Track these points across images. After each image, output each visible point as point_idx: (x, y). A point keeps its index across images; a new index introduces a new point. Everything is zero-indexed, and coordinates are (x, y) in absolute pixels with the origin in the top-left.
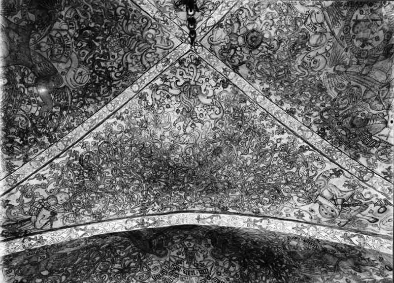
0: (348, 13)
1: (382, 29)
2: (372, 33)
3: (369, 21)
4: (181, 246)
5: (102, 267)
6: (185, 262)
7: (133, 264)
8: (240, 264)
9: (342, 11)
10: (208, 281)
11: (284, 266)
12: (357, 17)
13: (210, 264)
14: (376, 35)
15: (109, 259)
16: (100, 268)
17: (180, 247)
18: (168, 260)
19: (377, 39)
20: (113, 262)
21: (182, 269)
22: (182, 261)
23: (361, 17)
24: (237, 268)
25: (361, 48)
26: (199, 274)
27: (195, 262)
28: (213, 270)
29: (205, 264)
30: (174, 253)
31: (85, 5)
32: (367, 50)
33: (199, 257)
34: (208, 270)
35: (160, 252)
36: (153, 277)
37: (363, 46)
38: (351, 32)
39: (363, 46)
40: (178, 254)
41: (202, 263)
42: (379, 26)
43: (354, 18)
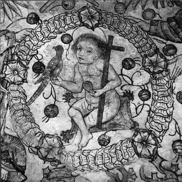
0: (132, 22)
1: (75, 126)
2: (68, 97)
3: (102, 87)
9: (140, 6)
12: (121, 49)
14: (63, 106)
19: (51, 111)
23: (116, 59)
25: (34, 61)
32: (24, 80)
37: (39, 68)
38: (84, 30)
39: (39, 68)
42: (84, 117)
43: (118, 40)
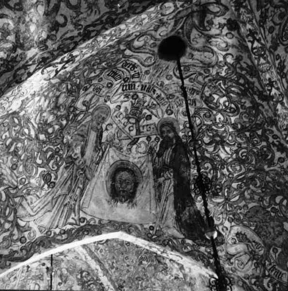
4: (141, 128)
5: (238, 168)
6: (146, 104)
7: (206, 140)
8: (76, 109)
10: (129, 77)
11: (12, 149)
13: (115, 98)
15: (225, 171)
16: (241, 169)
17: (143, 126)
18: (166, 116)
20: (223, 163)
21: (155, 96)
22: (148, 108)
24: (81, 100)
26: (137, 84)
27: (133, 101)
28: (116, 89)
29: (123, 96)
30: (155, 120)
31: (128, 246)
33: (126, 108)
34: (123, 90)
35: (169, 131)
36: (195, 105)
40: (149, 117)
41: (126, 99)
